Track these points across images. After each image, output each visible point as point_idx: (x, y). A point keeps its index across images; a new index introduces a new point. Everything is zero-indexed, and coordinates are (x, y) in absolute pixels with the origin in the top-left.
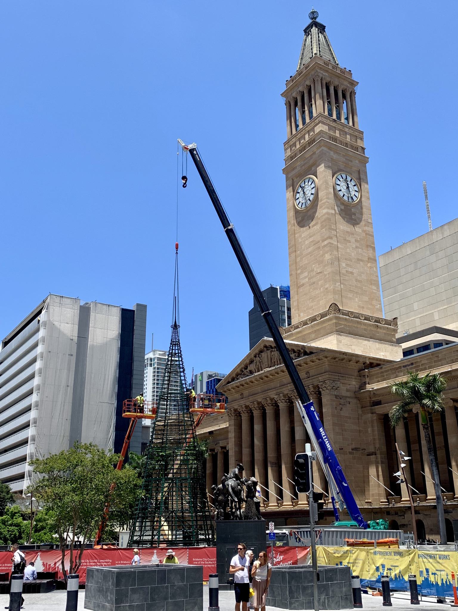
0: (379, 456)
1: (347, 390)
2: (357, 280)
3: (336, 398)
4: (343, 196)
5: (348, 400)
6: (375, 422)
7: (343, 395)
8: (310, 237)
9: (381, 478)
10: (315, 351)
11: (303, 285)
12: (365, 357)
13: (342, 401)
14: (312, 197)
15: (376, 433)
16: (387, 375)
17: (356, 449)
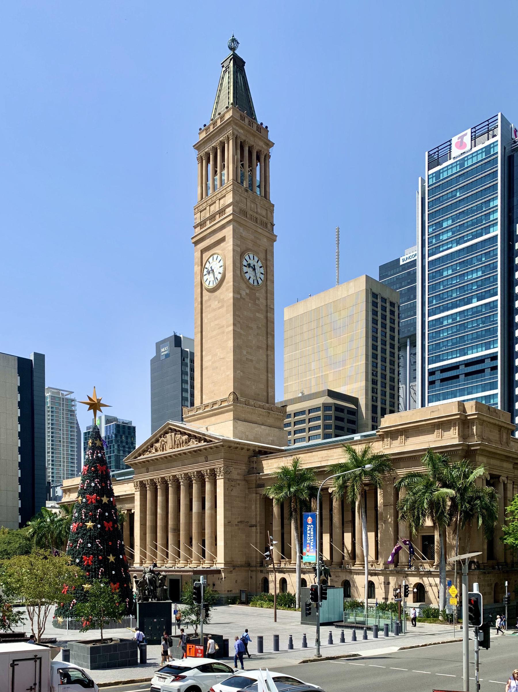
0: (258, 528)
1: (238, 474)
2: (255, 368)
3: (228, 481)
4: (249, 279)
5: (238, 482)
6: (258, 500)
7: (235, 478)
8: (216, 319)
9: (258, 545)
10: (214, 440)
11: (207, 367)
12: (255, 446)
13: (233, 483)
14: (219, 277)
15: (258, 509)
16: (271, 463)
17: (241, 522)
